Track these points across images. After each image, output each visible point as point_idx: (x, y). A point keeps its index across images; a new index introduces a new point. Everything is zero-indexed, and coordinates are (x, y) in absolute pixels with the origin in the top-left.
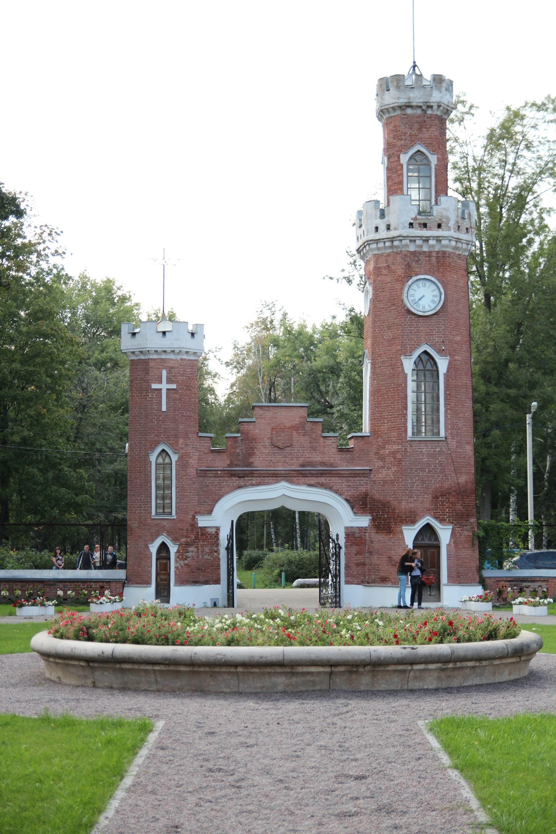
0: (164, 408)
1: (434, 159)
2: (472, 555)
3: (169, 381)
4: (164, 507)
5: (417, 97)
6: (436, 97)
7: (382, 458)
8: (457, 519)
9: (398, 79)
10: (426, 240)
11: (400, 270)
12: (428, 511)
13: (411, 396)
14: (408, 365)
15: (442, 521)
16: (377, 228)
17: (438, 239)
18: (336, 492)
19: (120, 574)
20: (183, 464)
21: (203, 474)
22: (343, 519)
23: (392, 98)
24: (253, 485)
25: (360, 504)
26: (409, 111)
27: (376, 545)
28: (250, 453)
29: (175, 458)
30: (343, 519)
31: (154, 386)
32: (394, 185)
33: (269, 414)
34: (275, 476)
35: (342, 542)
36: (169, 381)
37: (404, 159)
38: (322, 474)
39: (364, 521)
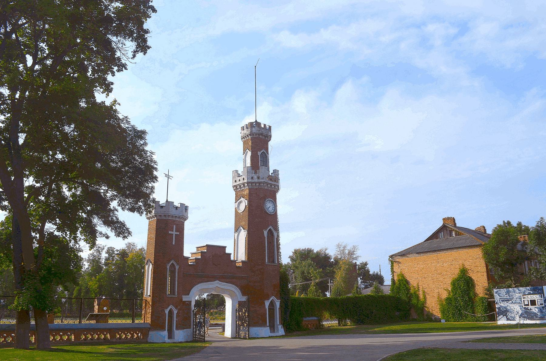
0: (174, 243)
10: (271, 185)
16: (252, 178)
18: (236, 285)
24: (206, 282)
26: (261, 136)
29: (177, 267)
31: (170, 232)
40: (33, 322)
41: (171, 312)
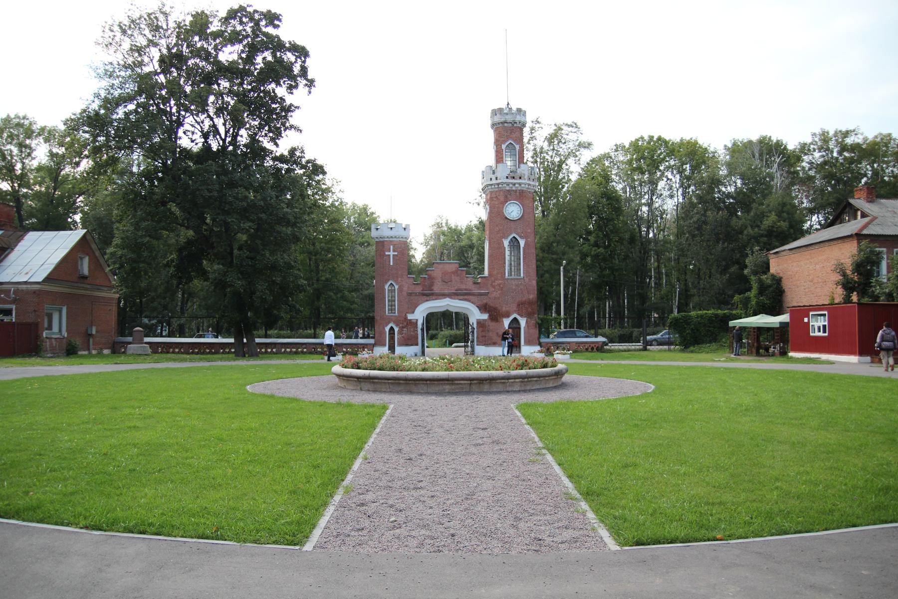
1: (517, 147)
2: (536, 332)
3: (394, 251)
4: (392, 310)
5: (509, 118)
6: (518, 118)
7: (494, 287)
8: (529, 315)
9: (500, 110)
10: (514, 184)
11: (502, 199)
12: (515, 312)
13: (507, 258)
14: (506, 243)
15: (521, 316)
17: (520, 184)
19: (372, 341)
20: (400, 290)
21: (410, 294)
22: (476, 315)
23: (498, 119)
25: (483, 308)
27: (491, 328)
28: (432, 285)
29: (397, 287)
30: (476, 315)
32: (499, 159)
33: (441, 266)
34: (444, 295)
35: (475, 326)
36: (394, 251)
37: (504, 147)
38: (466, 294)
39: (485, 316)
40: (245, 340)
41: (392, 329)
